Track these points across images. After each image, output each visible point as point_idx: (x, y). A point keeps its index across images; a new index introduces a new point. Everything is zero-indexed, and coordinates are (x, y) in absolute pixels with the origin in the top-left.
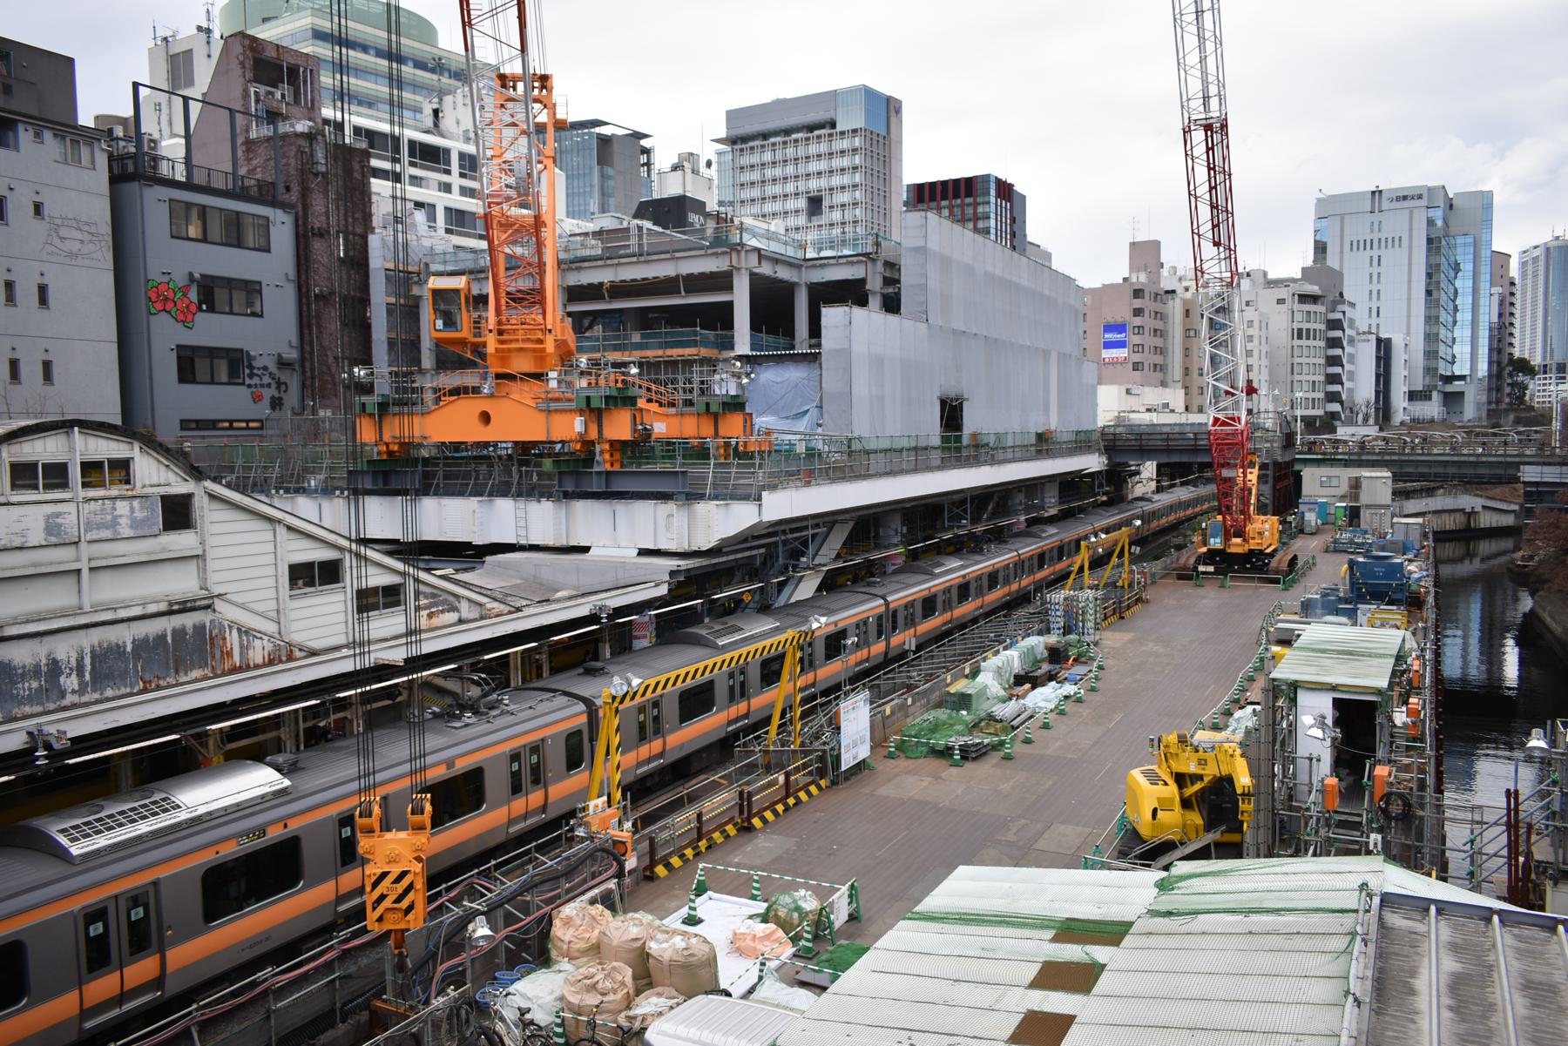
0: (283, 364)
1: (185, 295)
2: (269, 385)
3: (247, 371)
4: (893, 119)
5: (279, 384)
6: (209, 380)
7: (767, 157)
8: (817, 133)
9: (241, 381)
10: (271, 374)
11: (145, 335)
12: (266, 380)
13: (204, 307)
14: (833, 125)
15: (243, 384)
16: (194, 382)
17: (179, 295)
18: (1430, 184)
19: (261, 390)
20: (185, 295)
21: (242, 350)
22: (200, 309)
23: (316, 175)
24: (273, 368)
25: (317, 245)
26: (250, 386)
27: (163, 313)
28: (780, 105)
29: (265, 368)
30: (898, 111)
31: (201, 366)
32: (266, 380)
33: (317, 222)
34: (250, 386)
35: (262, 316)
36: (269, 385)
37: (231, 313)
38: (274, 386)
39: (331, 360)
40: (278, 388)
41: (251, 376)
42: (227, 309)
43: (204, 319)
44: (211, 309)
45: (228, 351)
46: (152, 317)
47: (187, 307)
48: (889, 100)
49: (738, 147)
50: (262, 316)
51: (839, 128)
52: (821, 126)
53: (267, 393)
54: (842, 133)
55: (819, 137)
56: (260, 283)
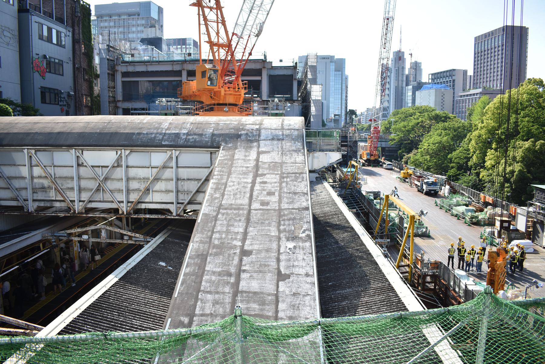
0: (69, 95)
1: (43, 64)
2: (65, 105)
3: (60, 99)
4: (160, 15)
5: (69, 106)
6: (49, 102)
7: (112, 24)
8: (132, 17)
9: (57, 103)
10: (66, 100)
11: (32, 81)
12: (65, 103)
13: (48, 70)
14: (139, 15)
15: (58, 104)
16: (45, 103)
17: (41, 64)
18: (331, 55)
19: (63, 107)
20: (43, 64)
21: (58, 90)
22: (47, 72)
23: (77, 17)
24: (66, 98)
25: (77, 47)
26: (60, 105)
27: (37, 72)
28: (115, 5)
29: (64, 98)
30: (162, 13)
31: (47, 95)
32: (65, 103)
33: (76, 37)
34: (60, 105)
35: (63, 75)
36: (65, 105)
37: (55, 73)
38: (67, 105)
39: (80, 95)
40: (68, 107)
41: (61, 101)
42: (53, 72)
43: (47, 74)
44: (50, 72)
45: (54, 89)
46: (34, 74)
47: (44, 70)
48: (159, 8)
49: (100, 19)
50: (63, 75)
51: (141, 16)
52: (134, 15)
53: (65, 108)
54: (143, 18)
55: (133, 19)
56: (62, 61)
